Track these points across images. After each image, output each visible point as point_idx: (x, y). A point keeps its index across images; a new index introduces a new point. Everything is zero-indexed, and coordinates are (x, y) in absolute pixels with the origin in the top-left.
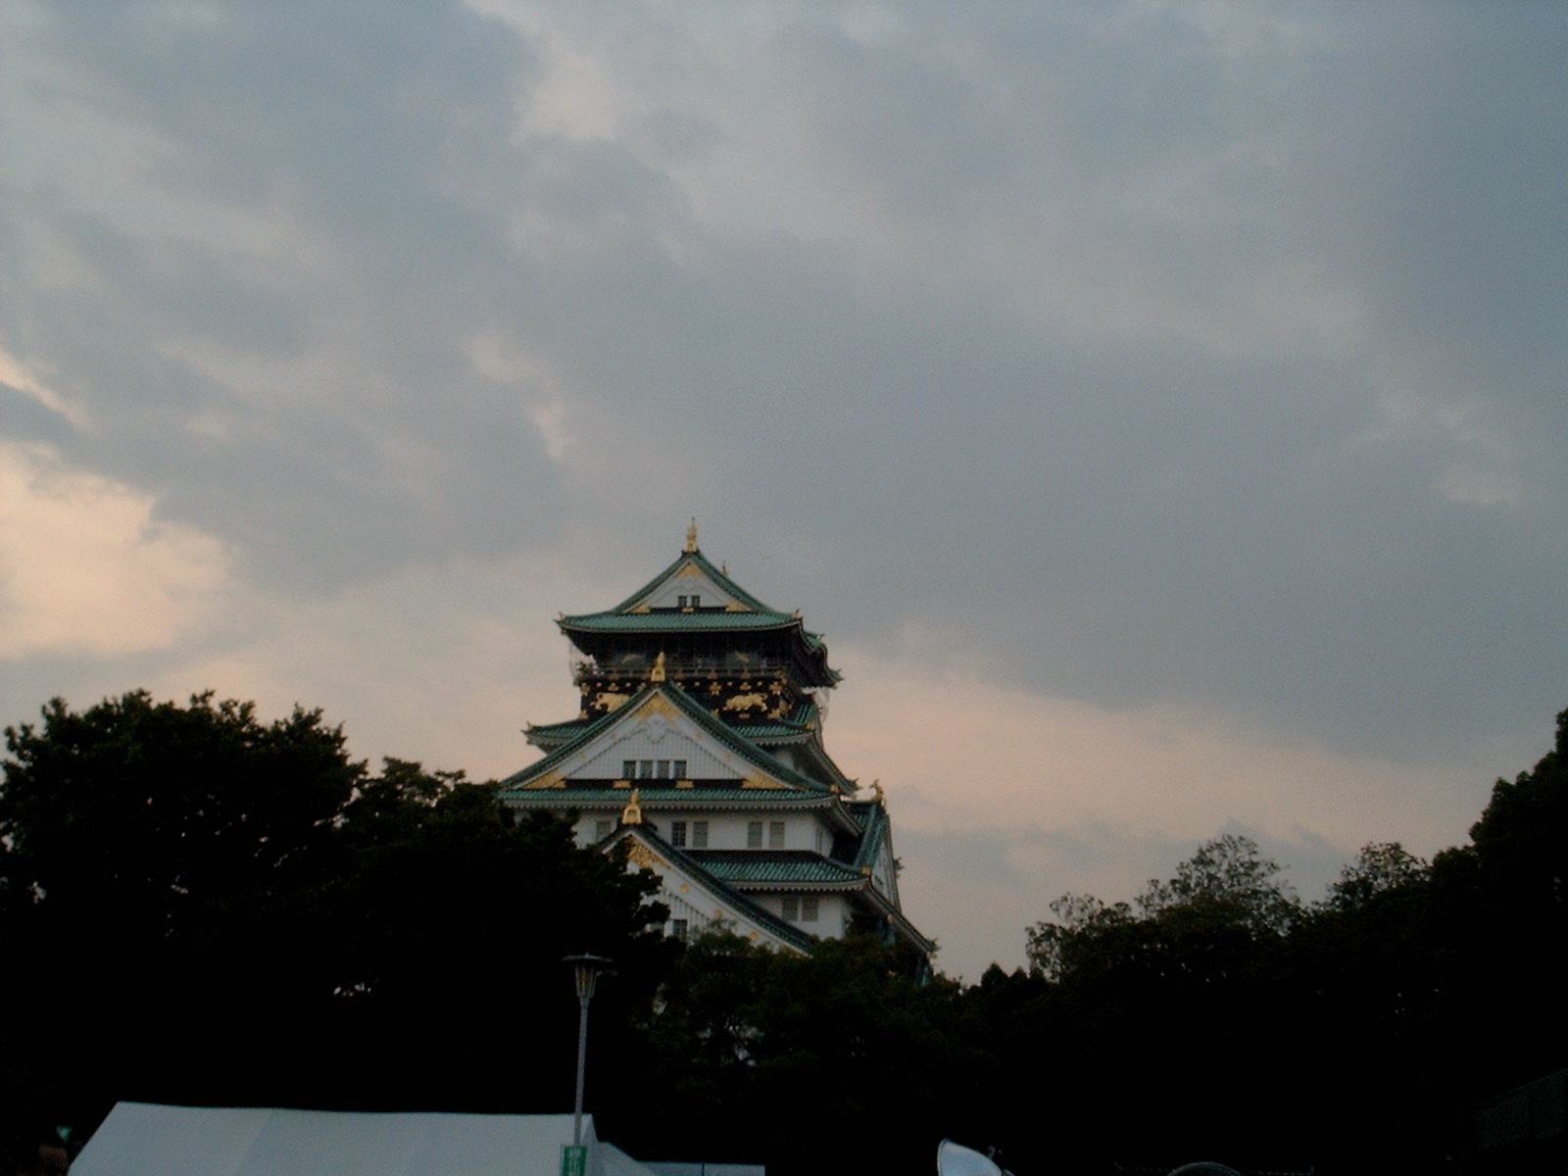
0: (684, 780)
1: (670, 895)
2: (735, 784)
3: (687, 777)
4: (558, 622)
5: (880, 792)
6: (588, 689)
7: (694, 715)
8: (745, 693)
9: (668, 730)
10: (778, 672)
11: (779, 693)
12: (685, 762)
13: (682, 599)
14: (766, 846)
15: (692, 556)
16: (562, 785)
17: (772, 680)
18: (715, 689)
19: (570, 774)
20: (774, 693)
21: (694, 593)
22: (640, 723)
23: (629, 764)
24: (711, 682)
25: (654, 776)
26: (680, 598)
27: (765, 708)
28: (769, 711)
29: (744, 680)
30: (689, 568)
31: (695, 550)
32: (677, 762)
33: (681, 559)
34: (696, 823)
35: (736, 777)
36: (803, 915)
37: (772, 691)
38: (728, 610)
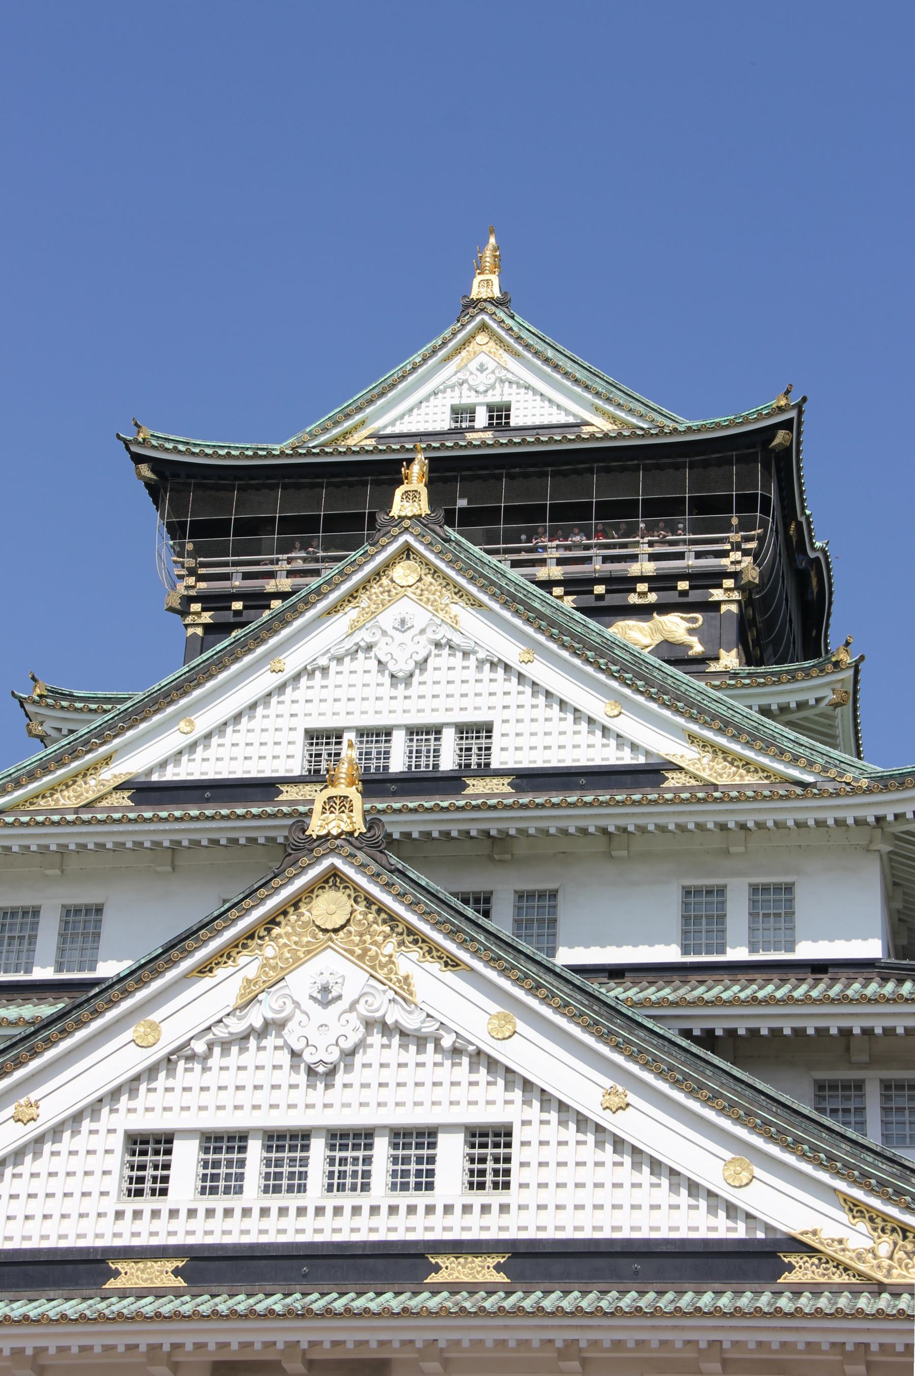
0: (485, 771)
1: (456, 1052)
4: (127, 443)
6: (207, 618)
7: (511, 600)
9: (438, 645)
10: (736, 556)
11: (734, 608)
12: (486, 729)
16: (123, 799)
17: (714, 578)
19: (150, 772)
20: (724, 608)
21: (494, 397)
22: (354, 628)
25: (397, 764)
26: (458, 412)
29: (642, 579)
30: (482, 338)
31: (497, 294)
32: (463, 730)
34: (520, 896)
35: (642, 760)
37: (717, 605)
38: (586, 429)
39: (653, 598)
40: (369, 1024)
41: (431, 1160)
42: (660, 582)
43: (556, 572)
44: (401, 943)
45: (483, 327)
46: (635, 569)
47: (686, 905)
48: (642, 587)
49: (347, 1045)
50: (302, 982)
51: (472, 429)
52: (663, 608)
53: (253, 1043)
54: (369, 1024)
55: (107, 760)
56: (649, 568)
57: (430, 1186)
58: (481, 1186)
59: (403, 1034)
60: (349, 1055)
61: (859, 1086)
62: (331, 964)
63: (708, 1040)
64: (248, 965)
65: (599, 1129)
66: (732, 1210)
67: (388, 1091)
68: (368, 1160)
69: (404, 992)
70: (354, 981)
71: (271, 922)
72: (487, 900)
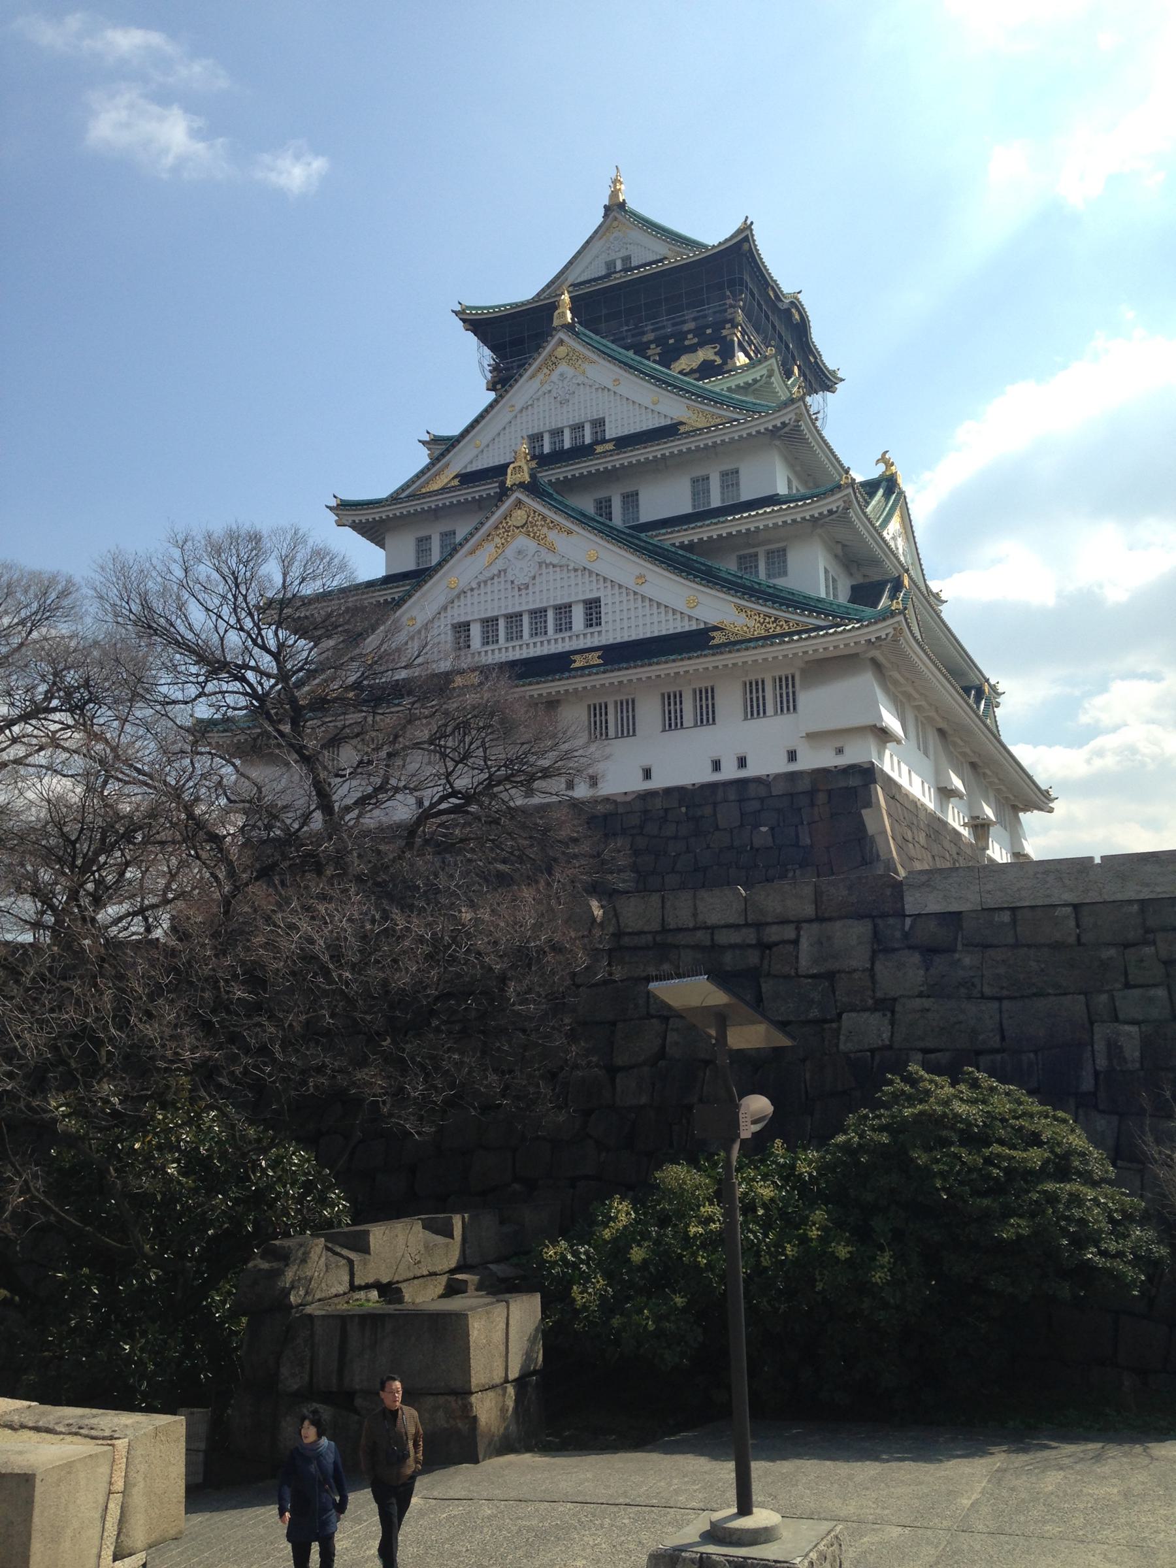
0: (604, 441)
2: (670, 431)
3: (607, 437)
5: (889, 464)
8: (692, 349)
13: (610, 265)
14: (716, 502)
15: (616, 209)
16: (456, 482)
18: (654, 350)
19: (466, 467)
23: (535, 439)
24: (647, 346)
25: (567, 445)
27: (719, 361)
28: (725, 363)
29: (689, 332)
30: (615, 224)
33: (606, 216)
36: (767, 569)
39: (696, 340)
40: (540, 564)
41: (570, 617)
42: (698, 331)
43: (651, 336)
44: (549, 528)
45: (616, 219)
46: (686, 327)
47: (693, 487)
48: (690, 336)
49: (532, 574)
50: (510, 551)
51: (616, 272)
52: (701, 345)
53: (496, 580)
54: (540, 564)
55: (447, 465)
56: (691, 325)
57: (571, 628)
58: (591, 625)
59: (554, 566)
60: (534, 578)
61: (756, 555)
62: (522, 541)
63: (682, 546)
64: (489, 549)
65: (635, 593)
66: (690, 618)
67: (551, 591)
68: (545, 622)
69: (552, 549)
70: (530, 545)
71: (497, 528)
72: (610, 500)
